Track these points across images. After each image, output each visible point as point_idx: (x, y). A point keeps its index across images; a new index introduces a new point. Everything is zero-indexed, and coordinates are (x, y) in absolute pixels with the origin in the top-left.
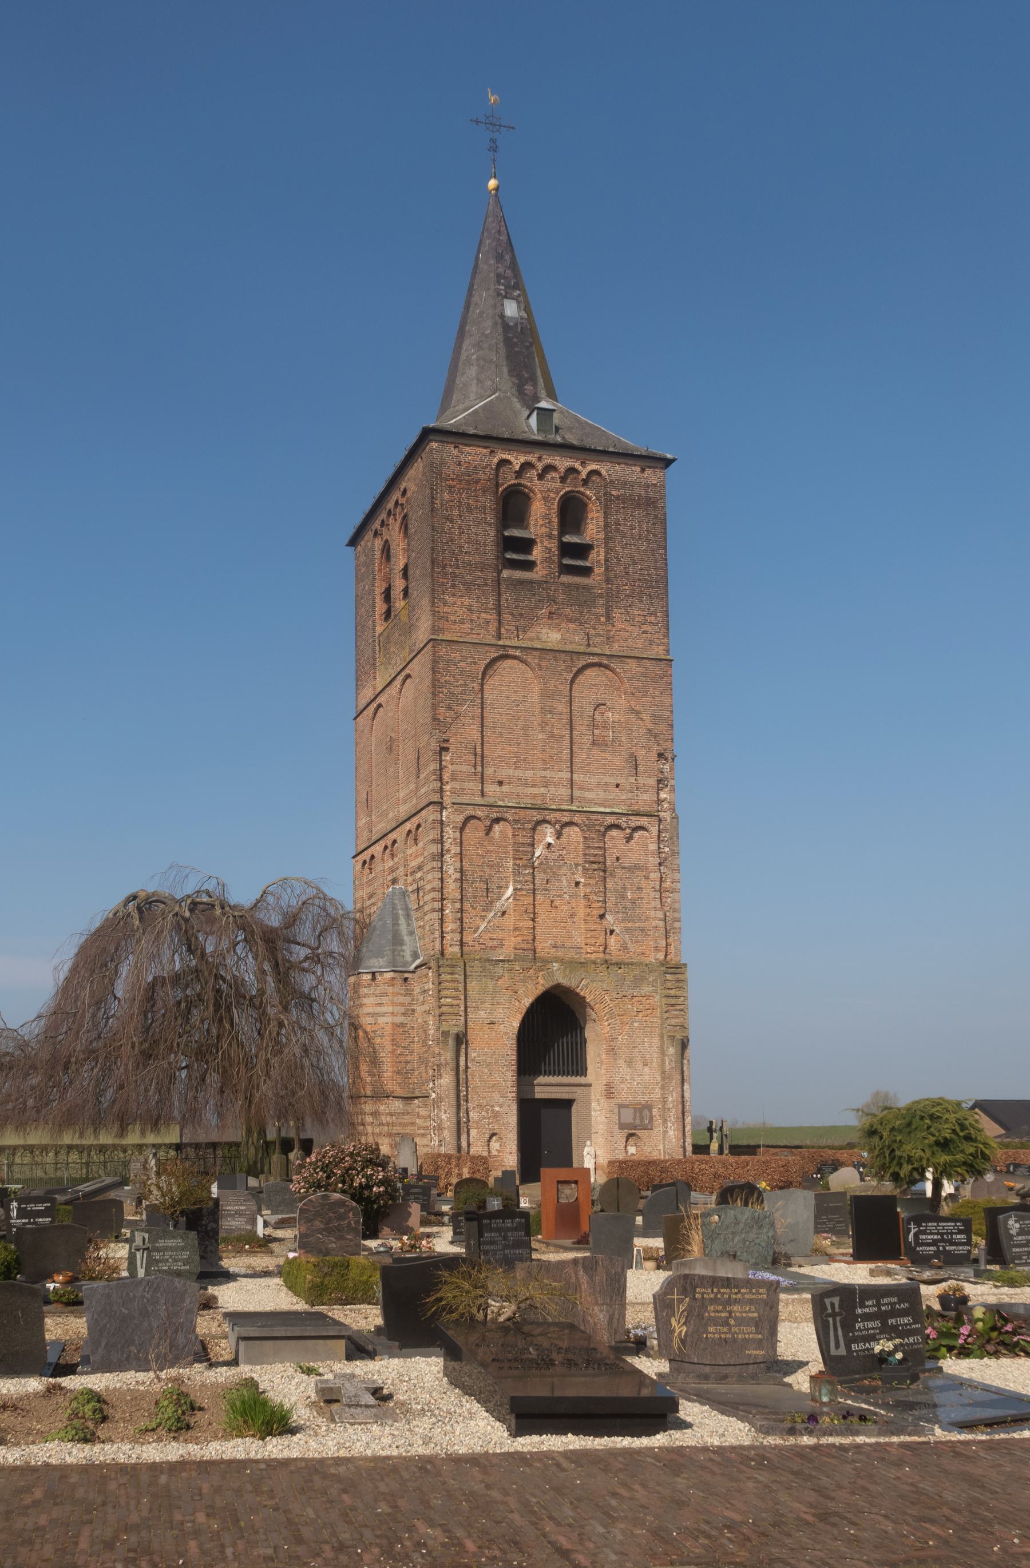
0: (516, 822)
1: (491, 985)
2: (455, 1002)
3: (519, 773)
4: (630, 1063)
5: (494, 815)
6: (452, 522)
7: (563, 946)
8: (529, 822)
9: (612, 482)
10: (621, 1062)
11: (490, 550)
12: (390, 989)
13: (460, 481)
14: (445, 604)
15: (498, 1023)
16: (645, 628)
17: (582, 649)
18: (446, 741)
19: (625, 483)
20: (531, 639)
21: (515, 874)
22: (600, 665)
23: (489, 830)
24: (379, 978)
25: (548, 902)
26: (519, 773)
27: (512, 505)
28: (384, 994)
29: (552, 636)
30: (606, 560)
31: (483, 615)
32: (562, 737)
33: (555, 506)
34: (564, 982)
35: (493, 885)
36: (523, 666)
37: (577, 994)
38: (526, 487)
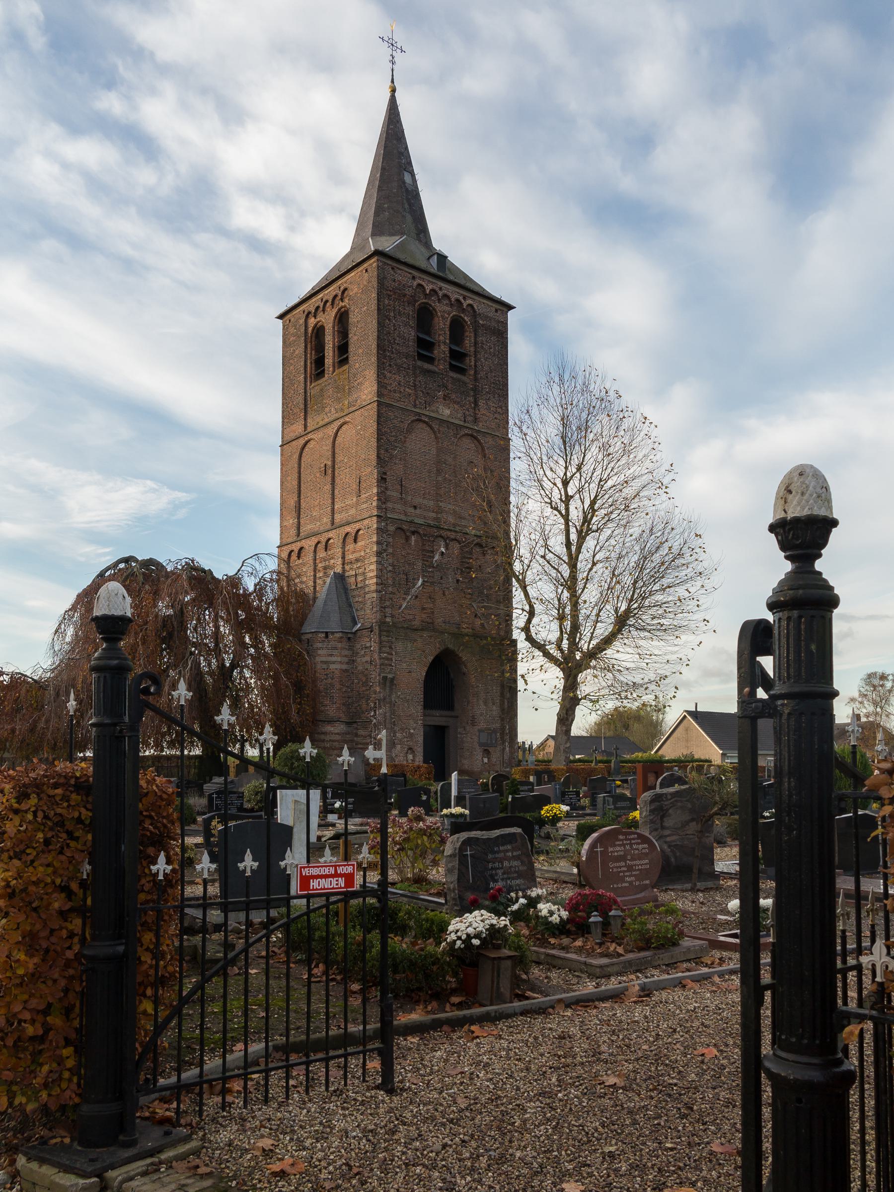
0: (425, 535)
1: (409, 645)
2: (390, 656)
3: (425, 502)
4: (485, 703)
5: (413, 529)
6: (389, 320)
7: (449, 622)
8: (432, 536)
9: (480, 314)
10: (481, 702)
11: (412, 344)
12: (339, 645)
13: (395, 293)
14: (385, 377)
15: (412, 670)
16: (496, 415)
17: (462, 423)
18: (385, 474)
19: (487, 317)
20: (433, 411)
21: (423, 571)
22: (472, 436)
23: (407, 539)
24: (331, 636)
25: (441, 592)
26: (425, 502)
27: (425, 317)
28: (336, 648)
29: (445, 412)
30: (476, 366)
31: (407, 389)
32: (450, 481)
33: (448, 323)
34: (451, 646)
35: (411, 577)
36: (428, 429)
37: (457, 655)
38: (431, 305)
